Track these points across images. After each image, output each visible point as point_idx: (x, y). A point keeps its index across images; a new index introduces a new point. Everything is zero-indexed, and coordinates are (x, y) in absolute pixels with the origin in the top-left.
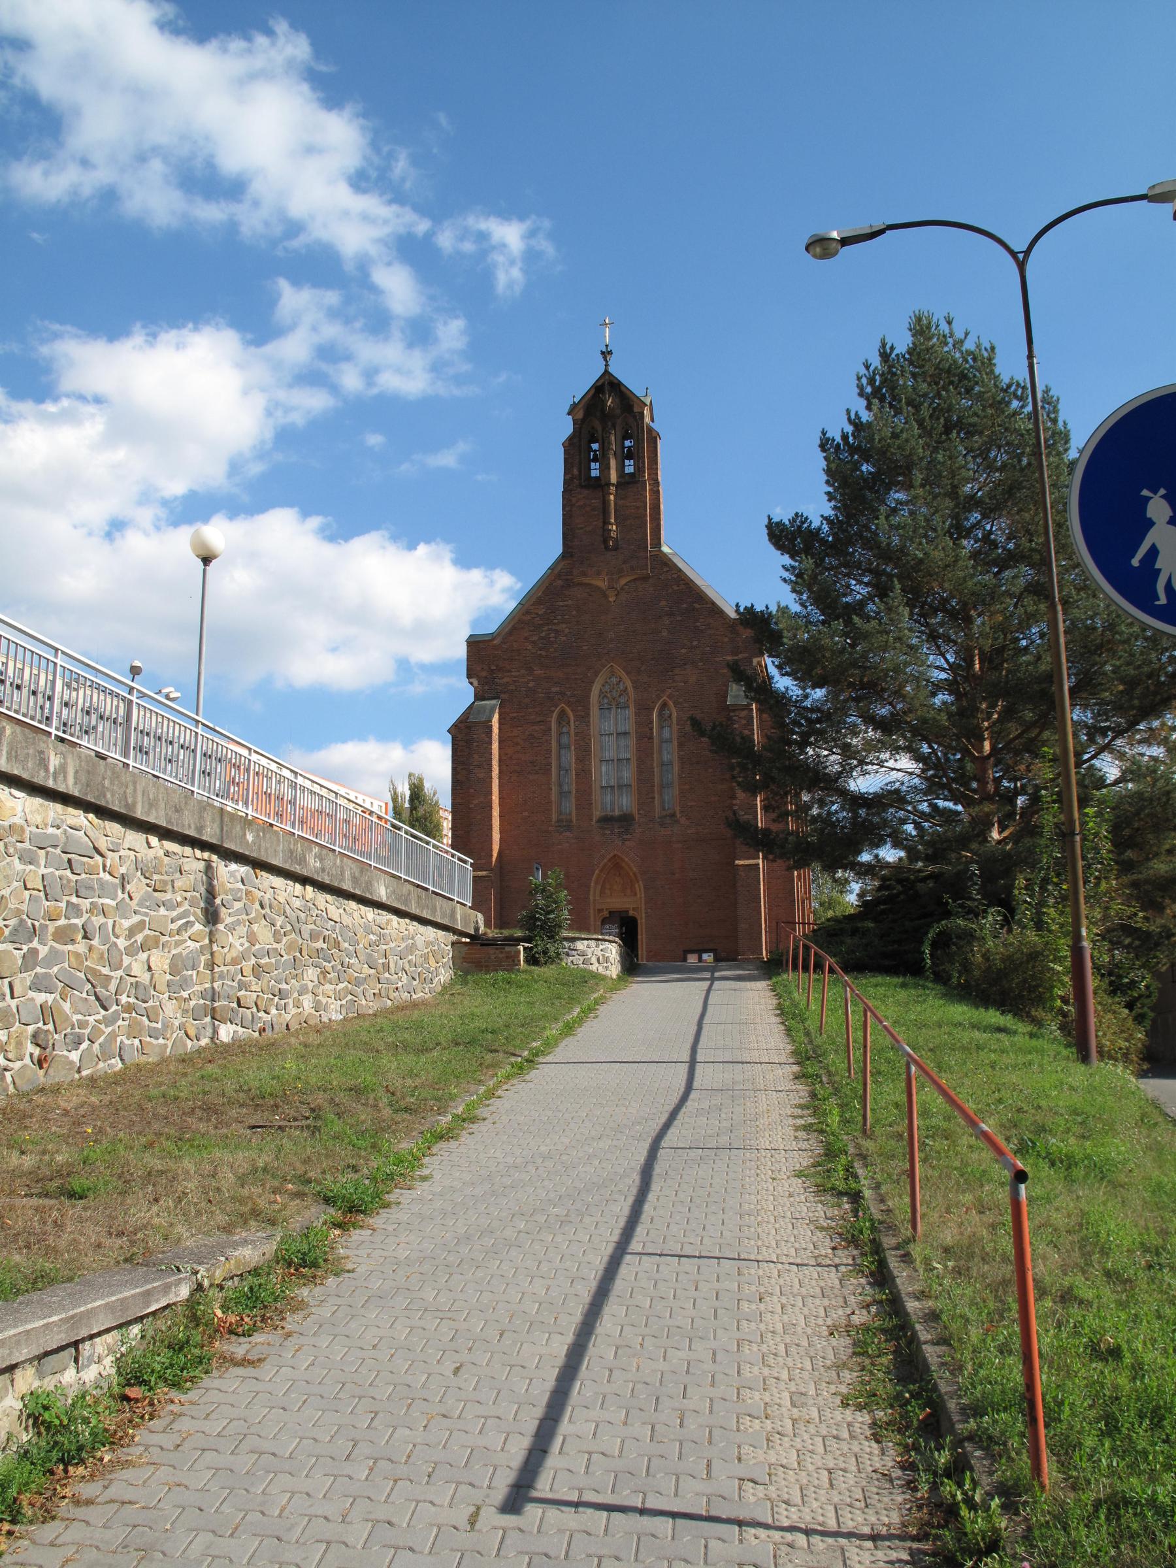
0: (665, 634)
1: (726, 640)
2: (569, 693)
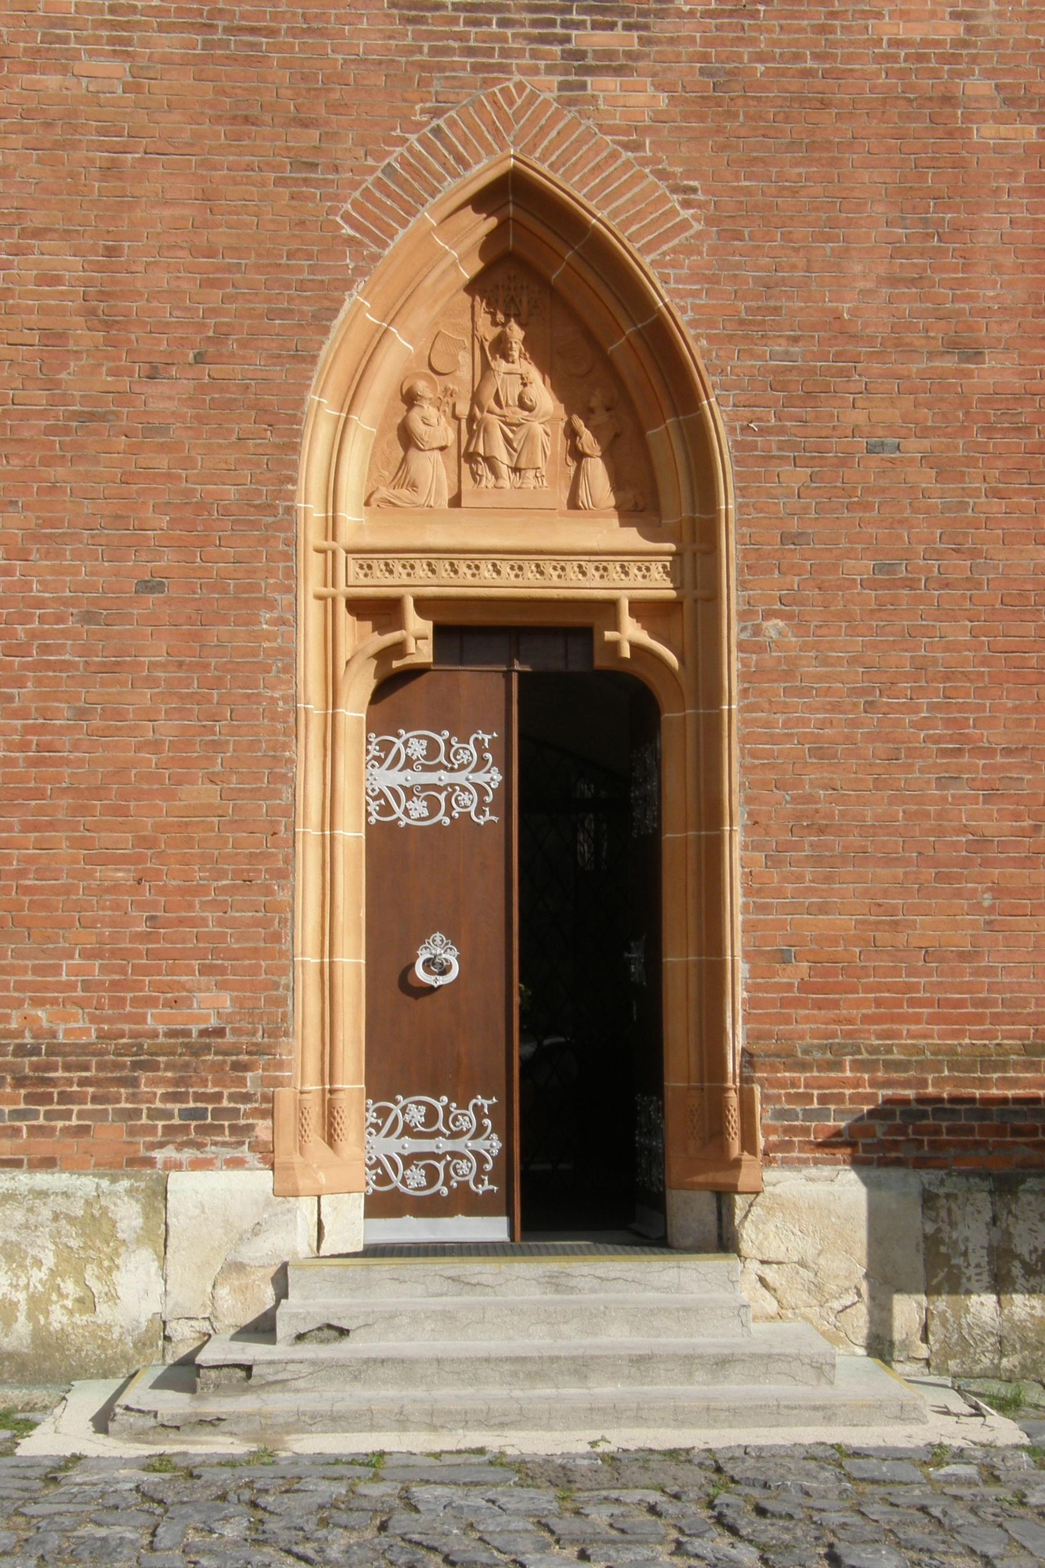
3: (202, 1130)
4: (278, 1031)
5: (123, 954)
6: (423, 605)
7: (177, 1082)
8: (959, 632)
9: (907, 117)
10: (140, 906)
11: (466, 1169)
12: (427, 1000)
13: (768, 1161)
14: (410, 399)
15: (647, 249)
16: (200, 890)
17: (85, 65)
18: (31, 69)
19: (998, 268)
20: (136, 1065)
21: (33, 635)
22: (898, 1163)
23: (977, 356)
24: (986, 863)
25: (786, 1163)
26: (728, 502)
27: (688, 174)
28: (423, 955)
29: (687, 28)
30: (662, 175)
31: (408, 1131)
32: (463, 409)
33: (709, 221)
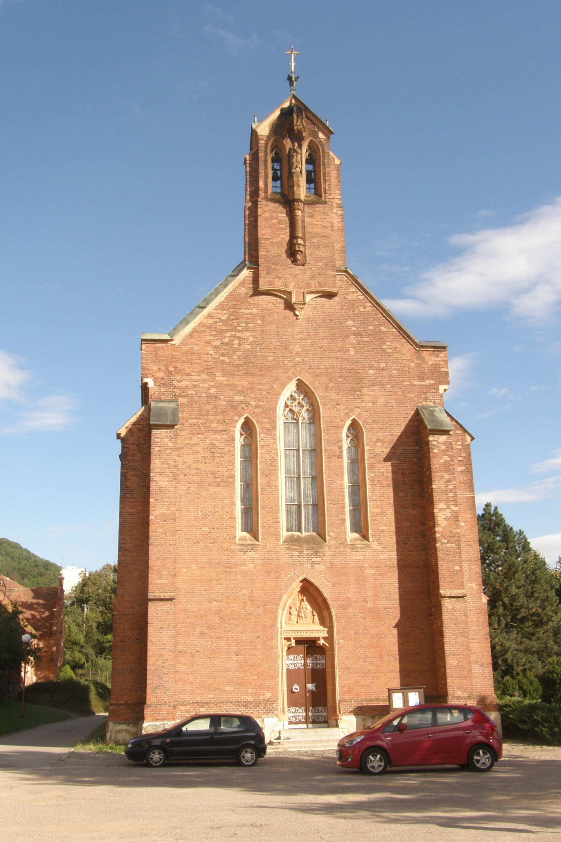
0: (352, 352)
1: (413, 365)
2: (253, 404)
3: (268, 712)
4: (277, 699)
5: (256, 688)
6: (294, 638)
7: (264, 706)
8: (366, 641)
9: (357, 570)
10: (258, 682)
11: (301, 718)
12: (294, 694)
13: (342, 715)
14: (290, 608)
15: (323, 589)
16: (266, 679)
17: (248, 565)
18: (241, 566)
19: (370, 590)
20: (259, 704)
21: (243, 644)
22: (360, 715)
23: (367, 602)
24: (370, 673)
25: (345, 715)
26: (335, 623)
27: (328, 578)
28: (294, 687)
29: (328, 558)
30: (325, 578)
31: (293, 712)
32: (298, 609)
33: (331, 584)
